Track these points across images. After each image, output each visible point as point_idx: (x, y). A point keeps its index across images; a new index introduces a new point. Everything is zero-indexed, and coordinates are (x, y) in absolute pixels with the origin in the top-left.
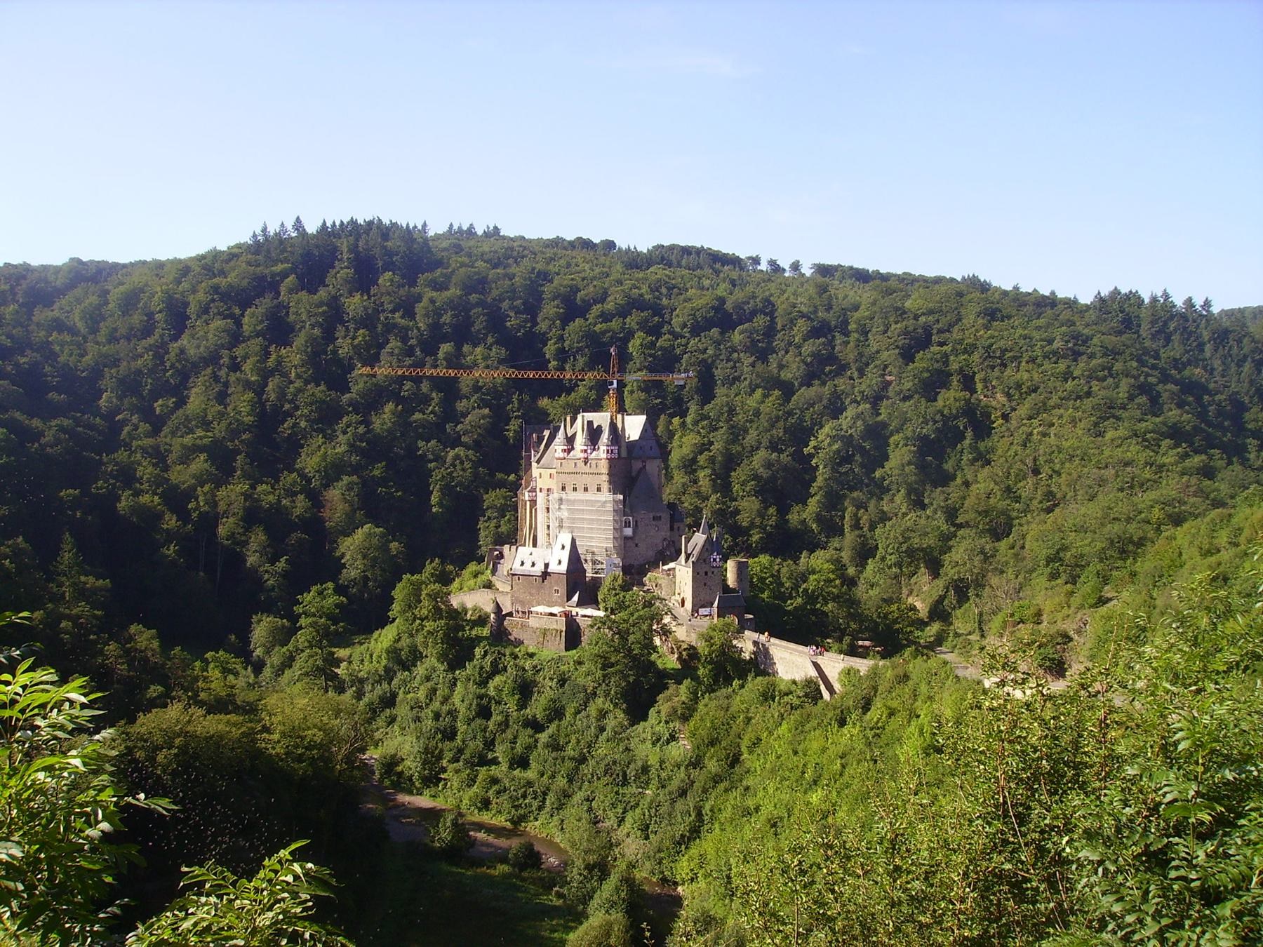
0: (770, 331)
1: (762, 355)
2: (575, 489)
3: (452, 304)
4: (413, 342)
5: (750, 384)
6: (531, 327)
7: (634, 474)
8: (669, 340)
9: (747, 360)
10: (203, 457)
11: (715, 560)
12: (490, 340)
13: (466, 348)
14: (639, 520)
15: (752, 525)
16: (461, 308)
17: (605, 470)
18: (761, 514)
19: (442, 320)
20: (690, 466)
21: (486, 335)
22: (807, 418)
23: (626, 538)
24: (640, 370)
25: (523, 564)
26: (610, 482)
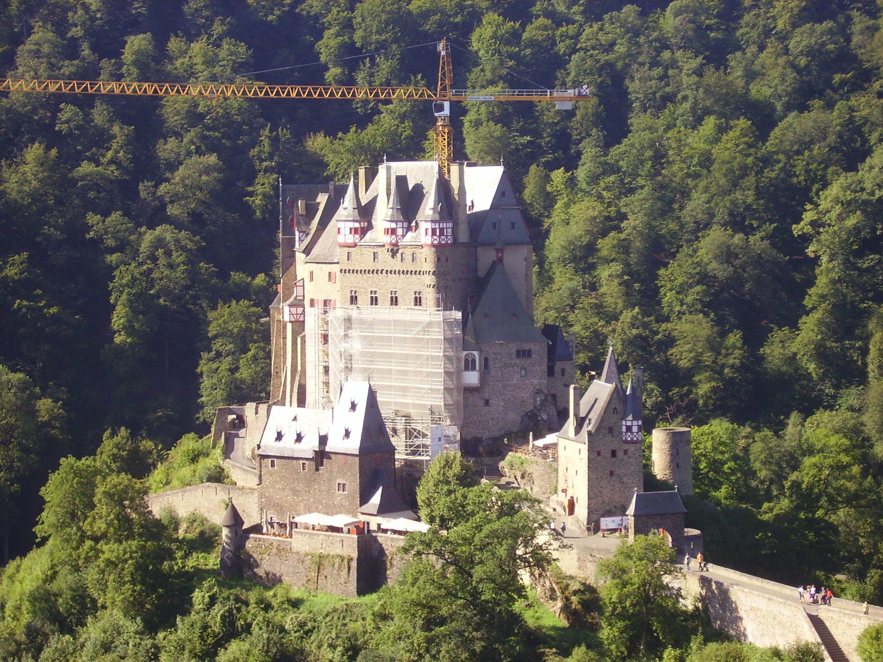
2: (374, 301)
4: (76, 32)
5: (693, 109)
7: (482, 273)
8: (546, 28)
9: (689, 62)
12: (218, 28)
13: (174, 44)
15: (698, 365)
17: (429, 266)
18: (715, 346)
21: (210, 20)
23: (469, 390)
24: (492, 83)
25: (279, 437)
26: (439, 288)
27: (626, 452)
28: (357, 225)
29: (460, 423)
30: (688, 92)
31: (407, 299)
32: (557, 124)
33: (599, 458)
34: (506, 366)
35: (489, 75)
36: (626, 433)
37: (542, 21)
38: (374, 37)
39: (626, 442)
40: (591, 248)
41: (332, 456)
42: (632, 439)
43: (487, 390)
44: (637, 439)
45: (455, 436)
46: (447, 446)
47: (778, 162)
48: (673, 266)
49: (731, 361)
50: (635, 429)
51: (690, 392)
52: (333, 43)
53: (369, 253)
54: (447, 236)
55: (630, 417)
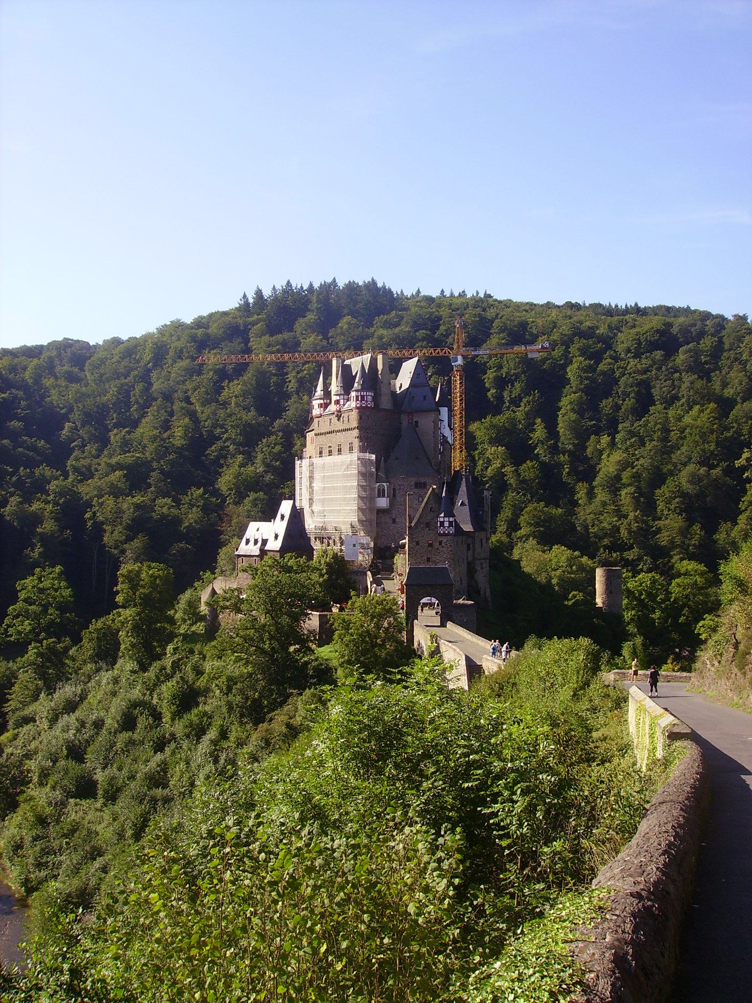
0: (717, 351)
1: (705, 374)
5: (688, 401)
8: (610, 364)
11: (442, 523)
14: (397, 487)
15: (672, 544)
18: (685, 532)
20: (614, 485)
22: (745, 432)
23: (380, 512)
27: (440, 543)
28: (322, 401)
29: (374, 534)
30: (684, 392)
32: (610, 414)
33: (418, 547)
36: (440, 527)
39: (440, 535)
40: (618, 478)
41: (268, 553)
42: (444, 532)
43: (394, 512)
44: (449, 532)
45: (368, 544)
46: (362, 551)
47: (733, 427)
48: (664, 488)
49: (693, 542)
50: (446, 524)
51: (669, 561)
52: (491, 376)
54: (367, 401)
55: (442, 515)
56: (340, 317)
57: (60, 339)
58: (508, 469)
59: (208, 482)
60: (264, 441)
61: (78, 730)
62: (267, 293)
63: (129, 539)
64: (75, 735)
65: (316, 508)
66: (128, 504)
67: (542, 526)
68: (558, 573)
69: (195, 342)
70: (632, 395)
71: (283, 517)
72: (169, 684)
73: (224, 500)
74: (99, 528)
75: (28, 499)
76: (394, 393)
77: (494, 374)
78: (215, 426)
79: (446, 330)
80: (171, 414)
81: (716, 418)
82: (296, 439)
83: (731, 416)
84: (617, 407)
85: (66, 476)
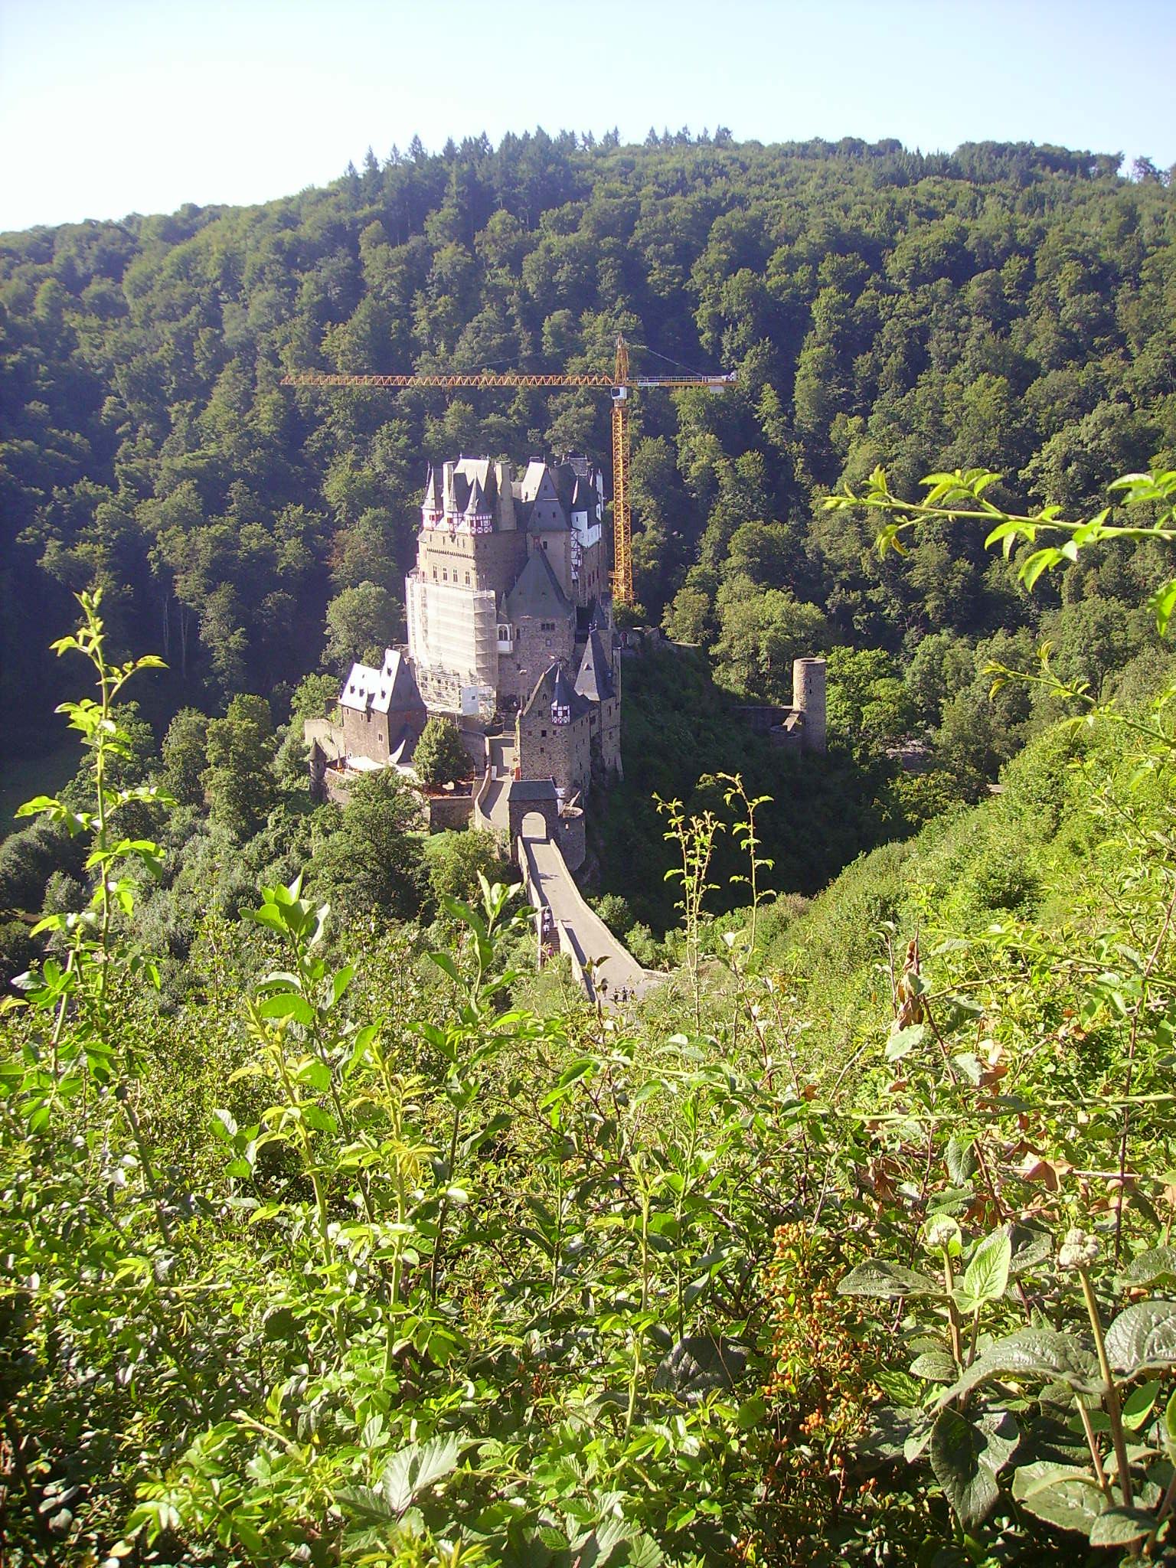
3: (572, 254)
4: (513, 310)
5: (972, 365)
6: (681, 284)
9: (979, 326)
10: (187, 485)
12: (619, 304)
13: (586, 317)
16: (586, 258)
17: (471, 553)
18: (946, 569)
19: (555, 278)
22: (1041, 422)
23: (501, 656)
24: (820, 345)
26: (478, 570)
31: (462, 578)
34: (532, 637)
35: (819, 338)
37: (872, 292)
38: (734, 309)
50: (560, 714)
52: (705, 314)
53: (440, 536)
56: (494, 209)
57: (78, 220)
58: (720, 464)
59: (308, 492)
60: (384, 428)
61: (179, 919)
62: (383, 158)
63: (210, 589)
64: (175, 925)
65: (432, 640)
66: (204, 537)
67: (758, 555)
68: (770, 632)
69: (282, 252)
70: (900, 349)
71: (389, 672)
72: (272, 868)
73: (333, 515)
74: (168, 573)
75: (70, 542)
76: (516, 502)
77: (710, 310)
78: (316, 402)
79: (643, 237)
80: (254, 381)
81: (1003, 400)
82: (428, 422)
83: (1028, 395)
84: (878, 368)
85: (115, 488)
